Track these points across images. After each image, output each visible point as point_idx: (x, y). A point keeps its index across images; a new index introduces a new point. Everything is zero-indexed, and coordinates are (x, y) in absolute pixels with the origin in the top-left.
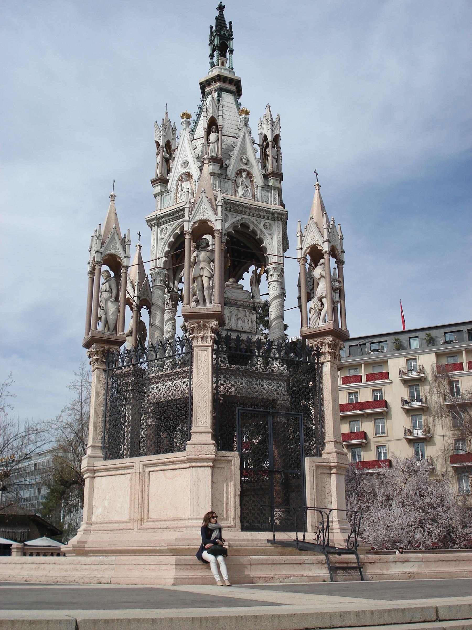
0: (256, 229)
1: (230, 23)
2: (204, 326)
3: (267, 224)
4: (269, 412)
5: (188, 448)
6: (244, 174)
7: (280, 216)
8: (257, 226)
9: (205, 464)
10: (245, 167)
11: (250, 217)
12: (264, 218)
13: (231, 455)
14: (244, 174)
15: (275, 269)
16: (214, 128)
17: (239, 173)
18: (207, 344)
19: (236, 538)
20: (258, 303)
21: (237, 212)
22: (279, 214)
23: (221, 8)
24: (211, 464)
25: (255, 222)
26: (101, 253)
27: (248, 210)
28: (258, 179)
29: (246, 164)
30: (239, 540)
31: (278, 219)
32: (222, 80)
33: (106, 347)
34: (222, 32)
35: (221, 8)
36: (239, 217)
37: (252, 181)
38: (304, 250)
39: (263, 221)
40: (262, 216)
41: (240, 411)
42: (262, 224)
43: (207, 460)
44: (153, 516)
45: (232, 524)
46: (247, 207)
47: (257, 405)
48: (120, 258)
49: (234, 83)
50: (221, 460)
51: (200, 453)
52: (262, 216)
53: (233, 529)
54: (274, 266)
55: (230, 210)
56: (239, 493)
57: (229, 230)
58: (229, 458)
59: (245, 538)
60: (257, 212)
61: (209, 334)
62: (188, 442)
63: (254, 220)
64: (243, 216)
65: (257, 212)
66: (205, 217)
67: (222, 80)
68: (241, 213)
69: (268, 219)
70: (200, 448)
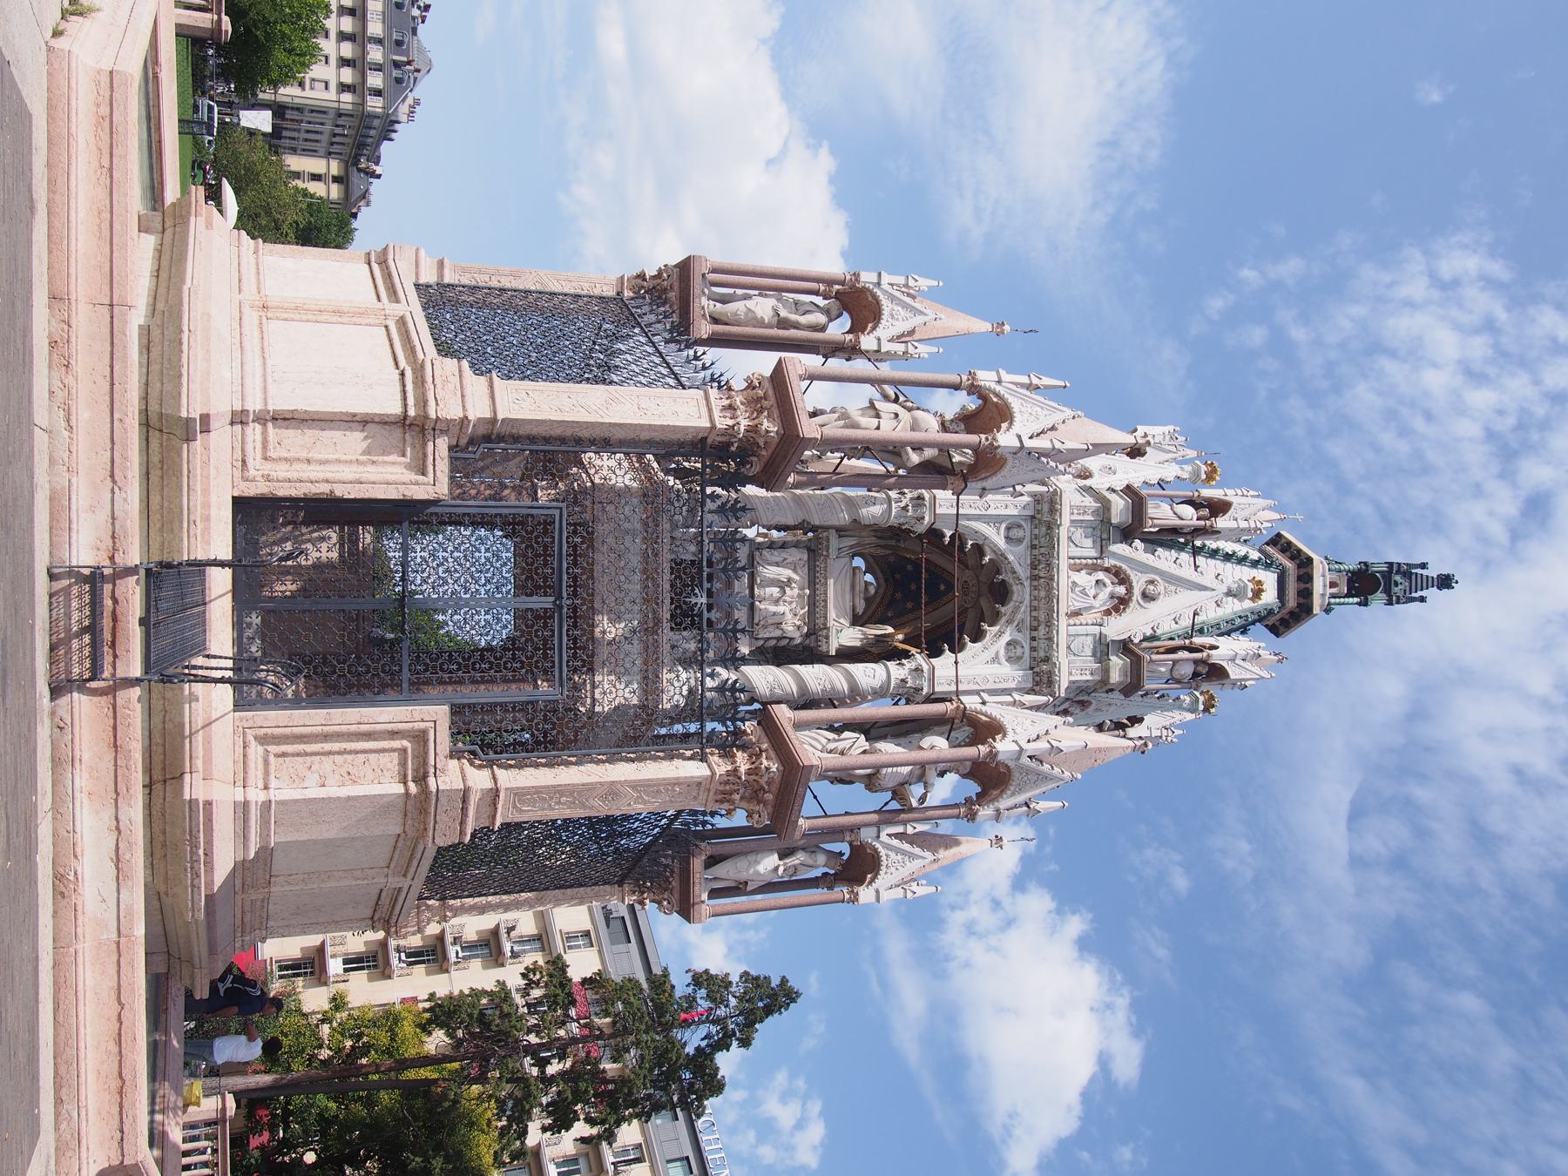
0: (1003, 620)
1: (1422, 599)
2: (760, 412)
3: (1019, 651)
4: (560, 597)
5: (451, 363)
6: (1121, 590)
7: (1045, 679)
8: (1009, 622)
9: (411, 401)
10: (1137, 592)
11: (1027, 602)
12: (1033, 639)
13: (438, 473)
14: (1121, 590)
15: (916, 669)
16: (1206, 512)
17: (1120, 577)
18: (716, 414)
19: (213, 472)
20: (827, 637)
21: (1034, 566)
22: (1050, 674)
23: (1445, 582)
24: (412, 412)
25: (1019, 616)
26: (879, 284)
27: (1043, 594)
28: (1117, 628)
29: (1145, 595)
30: (208, 477)
31: (1037, 674)
32: (1302, 571)
33: (672, 295)
34: (1398, 578)
35: (1445, 582)
36: (1023, 572)
37: (1108, 613)
38: (984, 709)
39: (1024, 639)
40: (1035, 634)
41: (557, 512)
42: (1019, 637)
43: (422, 402)
44: (273, 327)
45: (252, 472)
46: (1049, 589)
47: (575, 563)
48: (874, 329)
49: (1302, 601)
50: (424, 445)
51: (439, 386)
52: (1035, 634)
53: (238, 474)
54: (925, 667)
55: (1033, 547)
56: (338, 493)
57: (987, 549)
58: (430, 468)
59: (213, 498)
60: (1042, 617)
61: (744, 423)
62: (465, 363)
63: (1023, 613)
64: (1027, 583)
65: (1042, 617)
66: (1018, 417)
67: (1302, 571)
68: (1034, 578)
69: (1033, 649)
70: (451, 387)
